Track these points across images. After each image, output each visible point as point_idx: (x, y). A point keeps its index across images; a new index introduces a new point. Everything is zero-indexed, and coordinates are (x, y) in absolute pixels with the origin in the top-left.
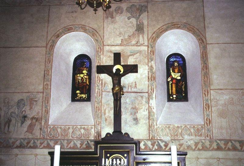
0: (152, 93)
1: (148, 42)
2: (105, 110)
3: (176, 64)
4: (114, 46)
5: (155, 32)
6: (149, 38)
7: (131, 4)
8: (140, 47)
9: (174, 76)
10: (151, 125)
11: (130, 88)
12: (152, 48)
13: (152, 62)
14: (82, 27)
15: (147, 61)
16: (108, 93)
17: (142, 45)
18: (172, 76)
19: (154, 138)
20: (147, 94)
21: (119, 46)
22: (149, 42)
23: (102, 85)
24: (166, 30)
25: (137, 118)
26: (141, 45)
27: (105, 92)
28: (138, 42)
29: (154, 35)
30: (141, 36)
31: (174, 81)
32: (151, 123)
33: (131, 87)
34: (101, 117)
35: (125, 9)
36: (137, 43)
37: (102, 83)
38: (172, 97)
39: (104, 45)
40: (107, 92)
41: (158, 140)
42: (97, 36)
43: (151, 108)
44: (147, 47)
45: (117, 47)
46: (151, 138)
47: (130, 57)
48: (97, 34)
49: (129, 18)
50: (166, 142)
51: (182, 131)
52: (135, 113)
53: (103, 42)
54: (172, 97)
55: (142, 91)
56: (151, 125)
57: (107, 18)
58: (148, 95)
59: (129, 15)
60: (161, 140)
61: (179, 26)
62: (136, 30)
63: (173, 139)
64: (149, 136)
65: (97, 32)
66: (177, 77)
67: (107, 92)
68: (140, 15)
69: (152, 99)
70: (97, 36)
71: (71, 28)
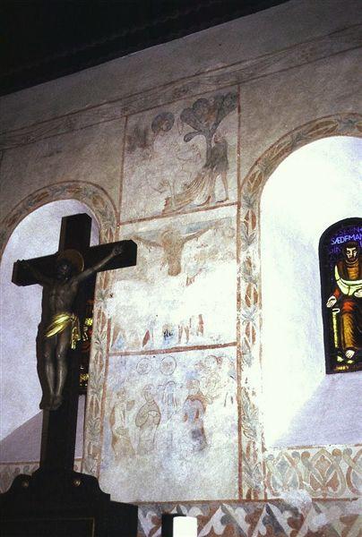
0: (250, 344)
1: (239, 192)
2: (113, 411)
3: (351, 252)
4: (144, 219)
5: (260, 159)
6: (242, 178)
7: (195, 99)
8: (214, 211)
9: (345, 290)
10: (245, 451)
11: (184, 334)
12: (250, 205)
13: (251, 248)
14: (69, 187)
15: (234, 248)
16: (123, 357)
17: (222, 204)
18: (340, 291)
19: (256, 496)
20: (233, 350)
21: (158, 217)
22: (242, 191)
23: (109, 335)
24: (292, 147)
25: (203, 429)
26: (218, 204)
27: (115, 354)
28: (210, 197)
29: (257, 169)
30: (219, 178)
31: (347, 306)
32: (244, 445)
33: (187, 331)
34: (102, 431)
35: (177, 116)
36: (207, 202)
37: (109, 329)
38: (343, 355)
39: (119, 223)
40: (121, 355)
41: (271, 501)
42: (103, 203)
43: (247, 394)
44: (233, 211)
45: (155, 221)
46: (244, 498)
47: (188, 244)
48: (106, 198)
49: (187, 139)
50: (296, 509)
51: (350, 468)
52: (198, 413)
53: (118, 216)
54: (343, 355)
55: (218, 342)
56: (245, 451)
57: (132, 149)
58: (238, 352)
59: (188, 128)
60: (278, 503)
61: (331, 126)
62: (206, 166)
63: (318, 500)
64: (240, 489)
65: (106, 193)
66: (357, 291)
67: (121, 355)
68: (217, 124)
69: (249, 364)
70: (103, 203)
71: (42, 194)
